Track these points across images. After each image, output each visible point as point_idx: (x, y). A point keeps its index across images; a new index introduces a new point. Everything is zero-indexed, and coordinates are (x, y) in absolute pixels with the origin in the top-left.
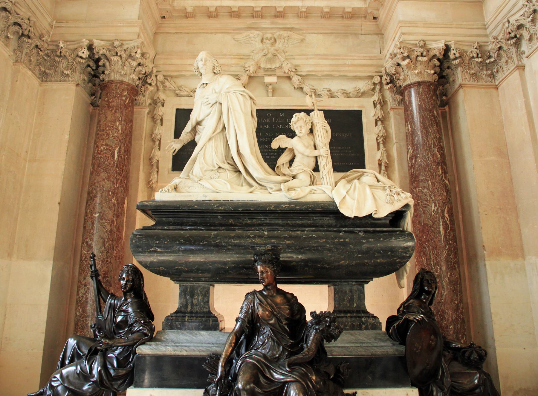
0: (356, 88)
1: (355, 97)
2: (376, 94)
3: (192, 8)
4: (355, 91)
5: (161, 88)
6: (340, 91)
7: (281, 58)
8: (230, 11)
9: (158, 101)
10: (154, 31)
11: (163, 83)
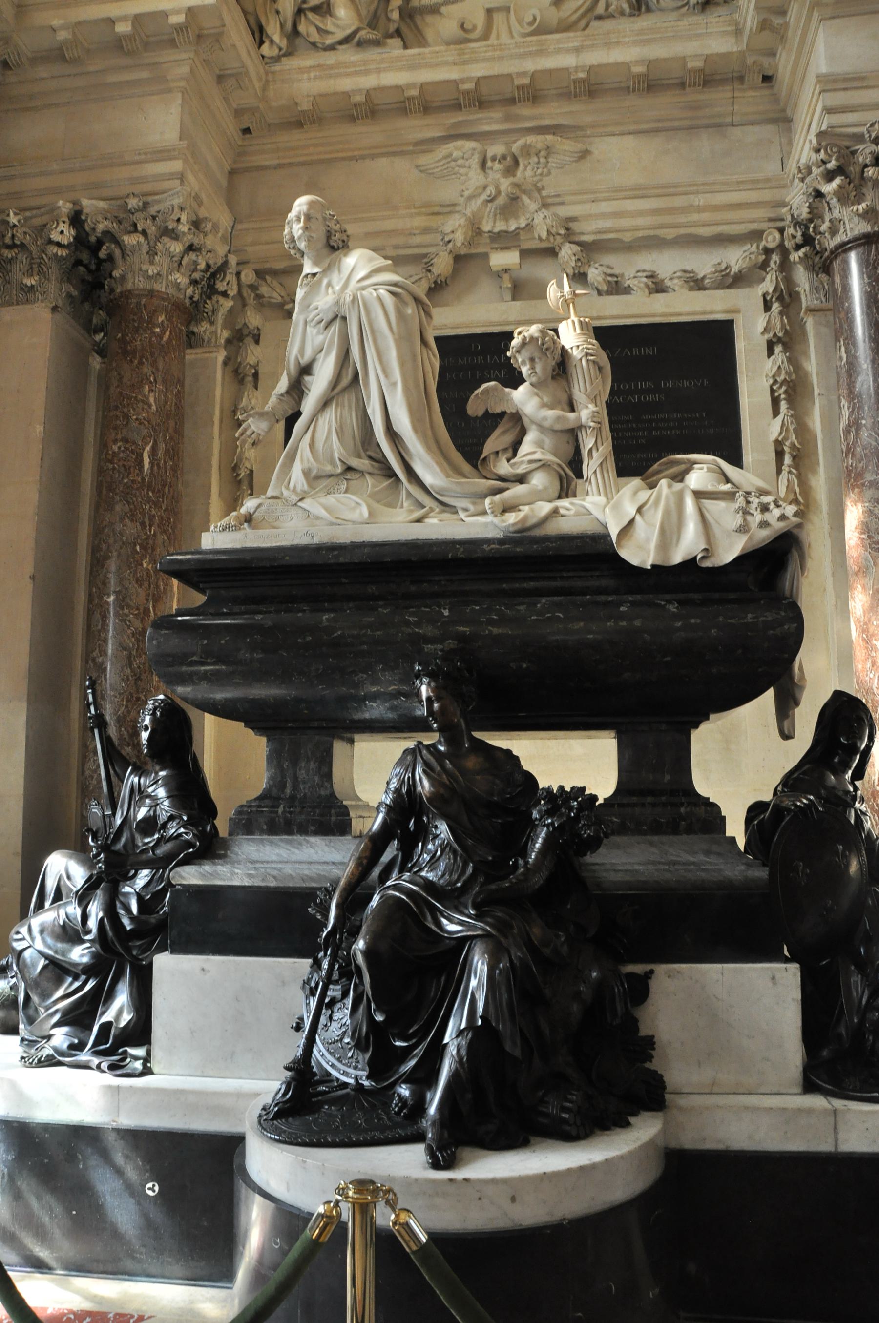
0: (719, 264)
1: (717, 288)
2: (768, 277)
3: (311, 99)
4: (716, 272)
5: (251, 300)
6: (678, 274)
7: (530, 204)
8: (402, 99)
9: (245, 332)
10: (227, 168)
11: (253, 287)
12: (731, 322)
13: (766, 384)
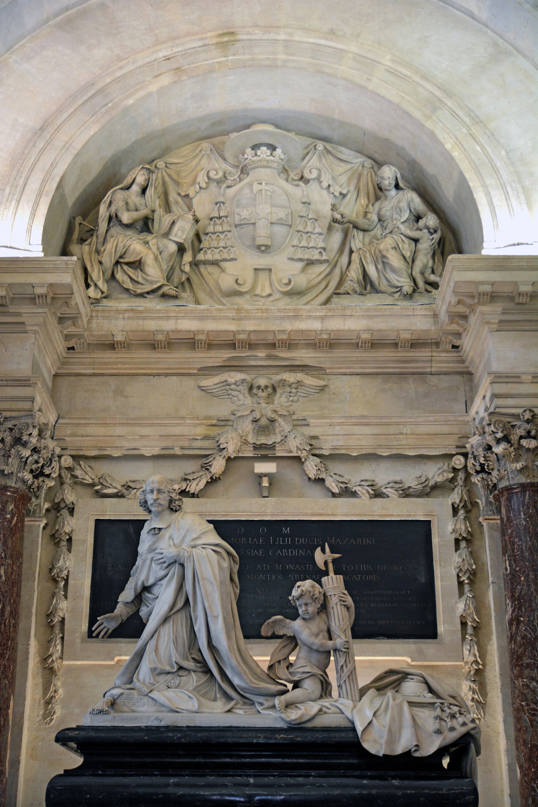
2: (456, 490)
6: (391, 485)
12: (429, 522)
13: (454, 572)
